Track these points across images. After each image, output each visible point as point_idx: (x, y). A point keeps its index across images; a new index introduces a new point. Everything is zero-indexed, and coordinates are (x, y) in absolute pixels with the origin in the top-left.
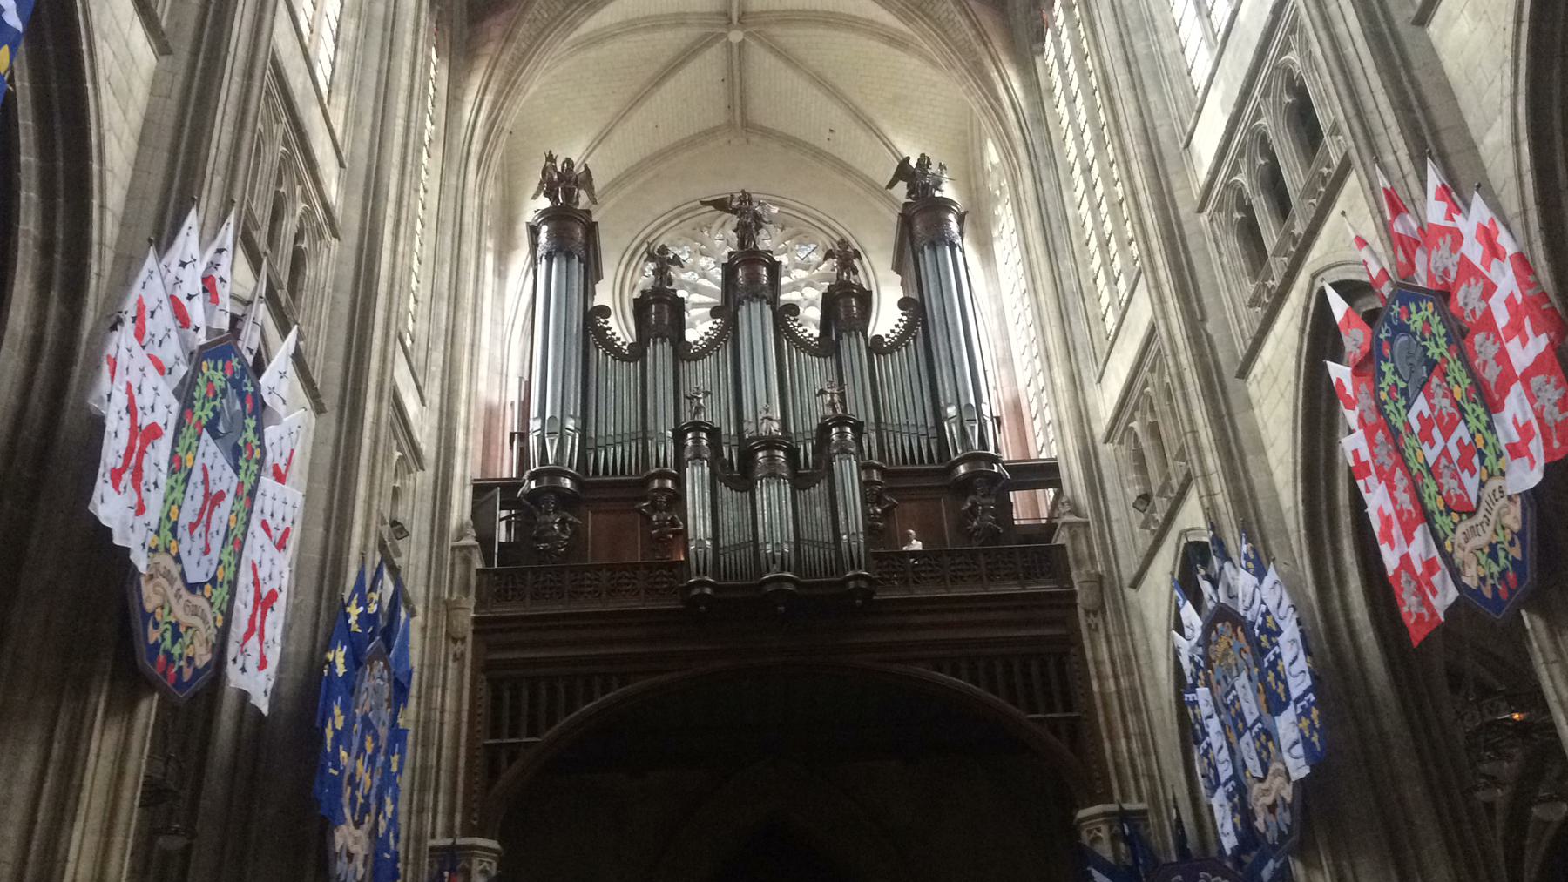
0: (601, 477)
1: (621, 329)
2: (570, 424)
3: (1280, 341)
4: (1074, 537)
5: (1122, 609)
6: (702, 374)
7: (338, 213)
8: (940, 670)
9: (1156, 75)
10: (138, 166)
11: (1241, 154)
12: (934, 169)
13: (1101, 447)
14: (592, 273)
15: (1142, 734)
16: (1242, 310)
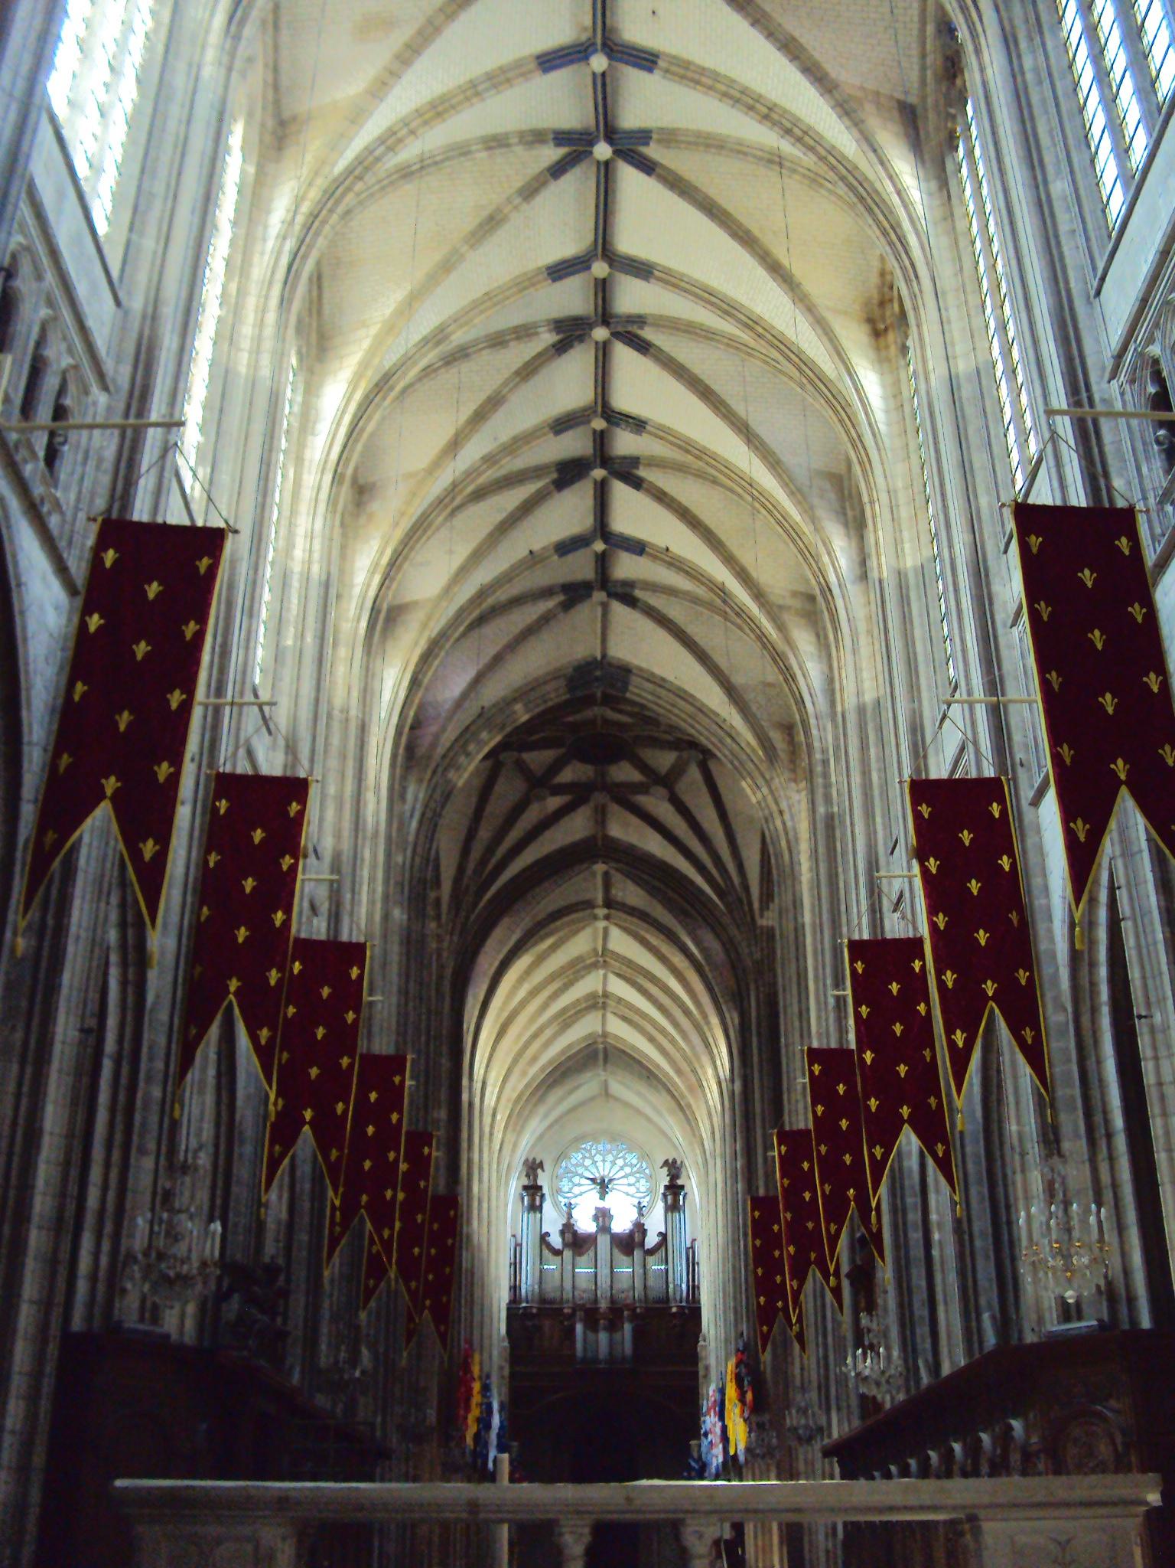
1: (556, 1241)
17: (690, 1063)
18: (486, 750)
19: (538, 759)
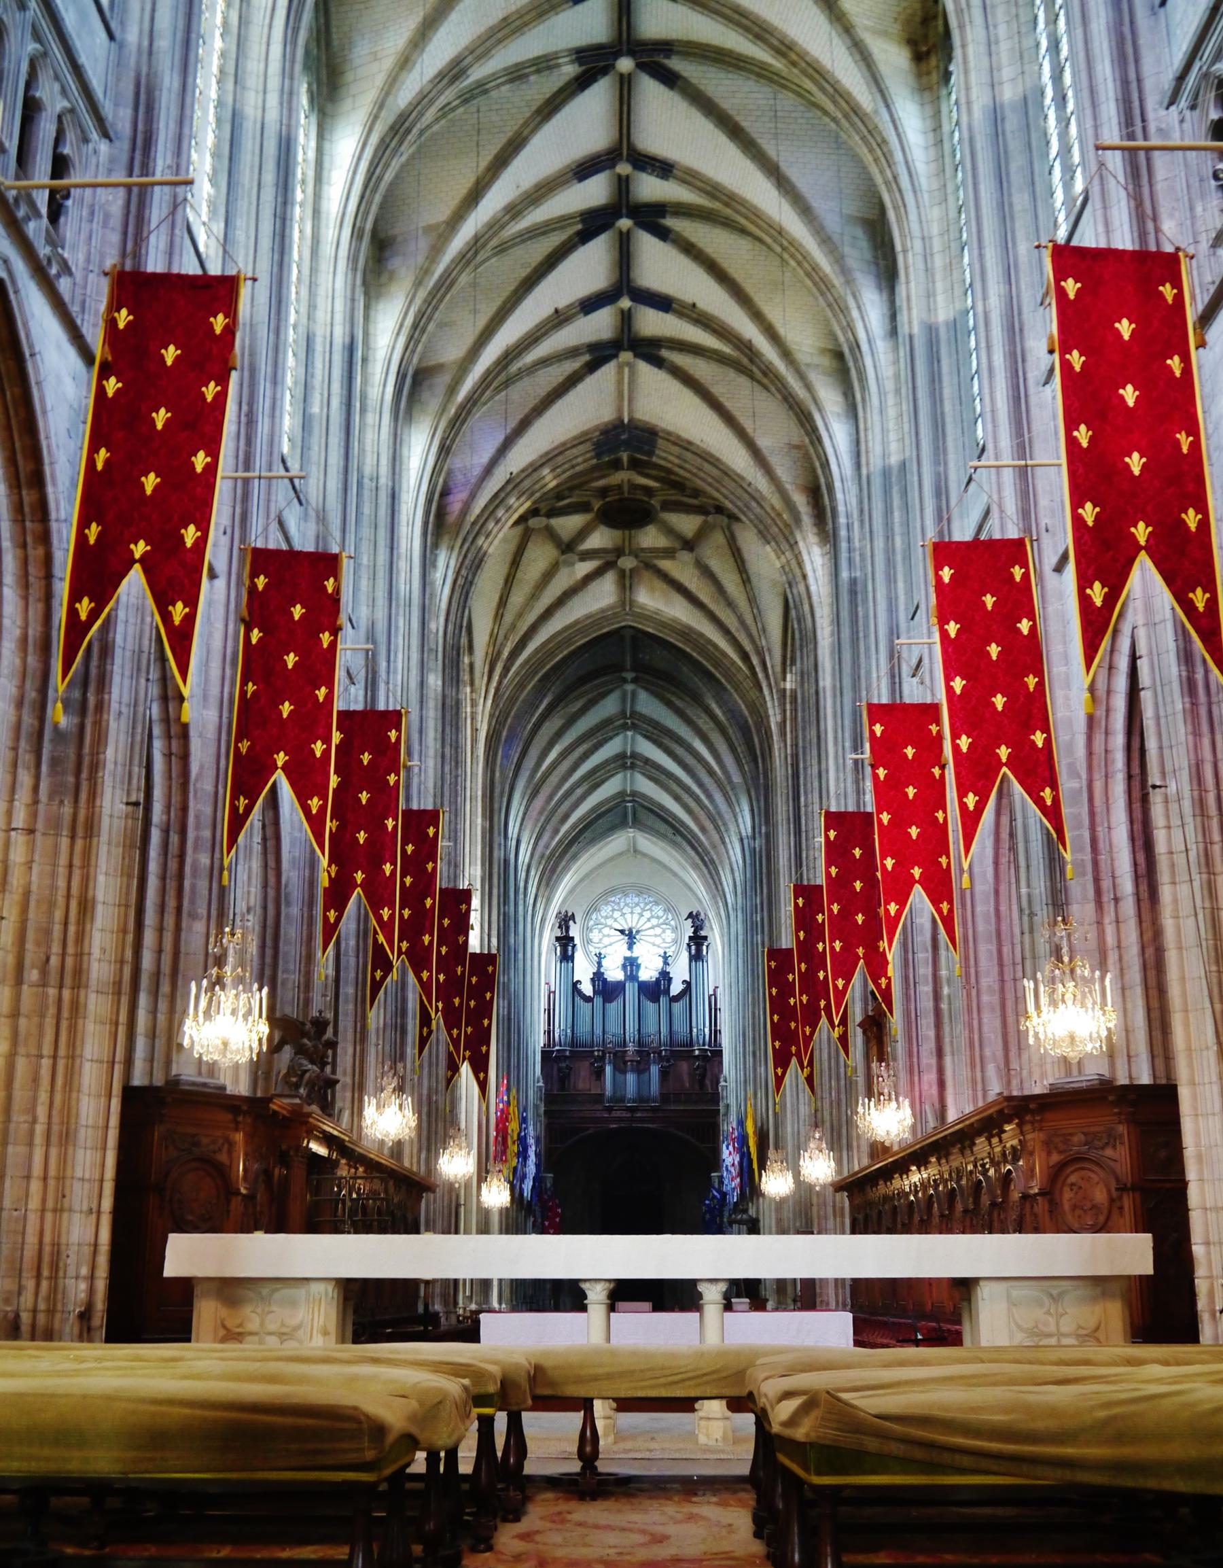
17: (713, 821)
18: (516, 516)
19: (568, 524)
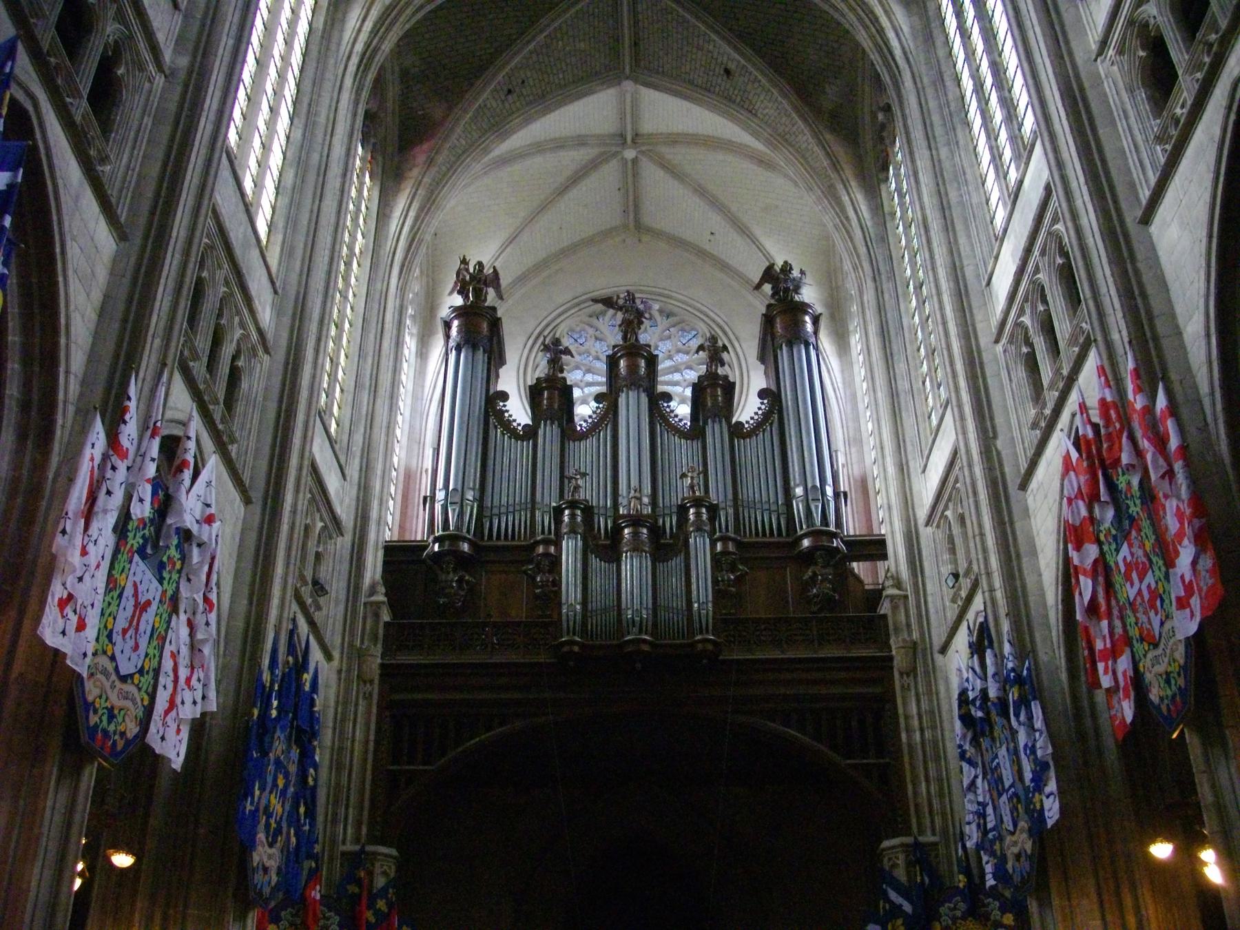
0: (494, 543)
1: (518, 411)
2: (470, 495)
3: (1049, 464)
4: (895, 608)
5: (931, 672)
6: (585, 454)
7: (270, 336)
8: (774, 721)
9: (965, 220)
10: (97, 335)
11: (1026, 300)
12: (795, 273)
13: (921, 528)
14: (496, 358)
15: (940, 780)
16: (1026, 431)
